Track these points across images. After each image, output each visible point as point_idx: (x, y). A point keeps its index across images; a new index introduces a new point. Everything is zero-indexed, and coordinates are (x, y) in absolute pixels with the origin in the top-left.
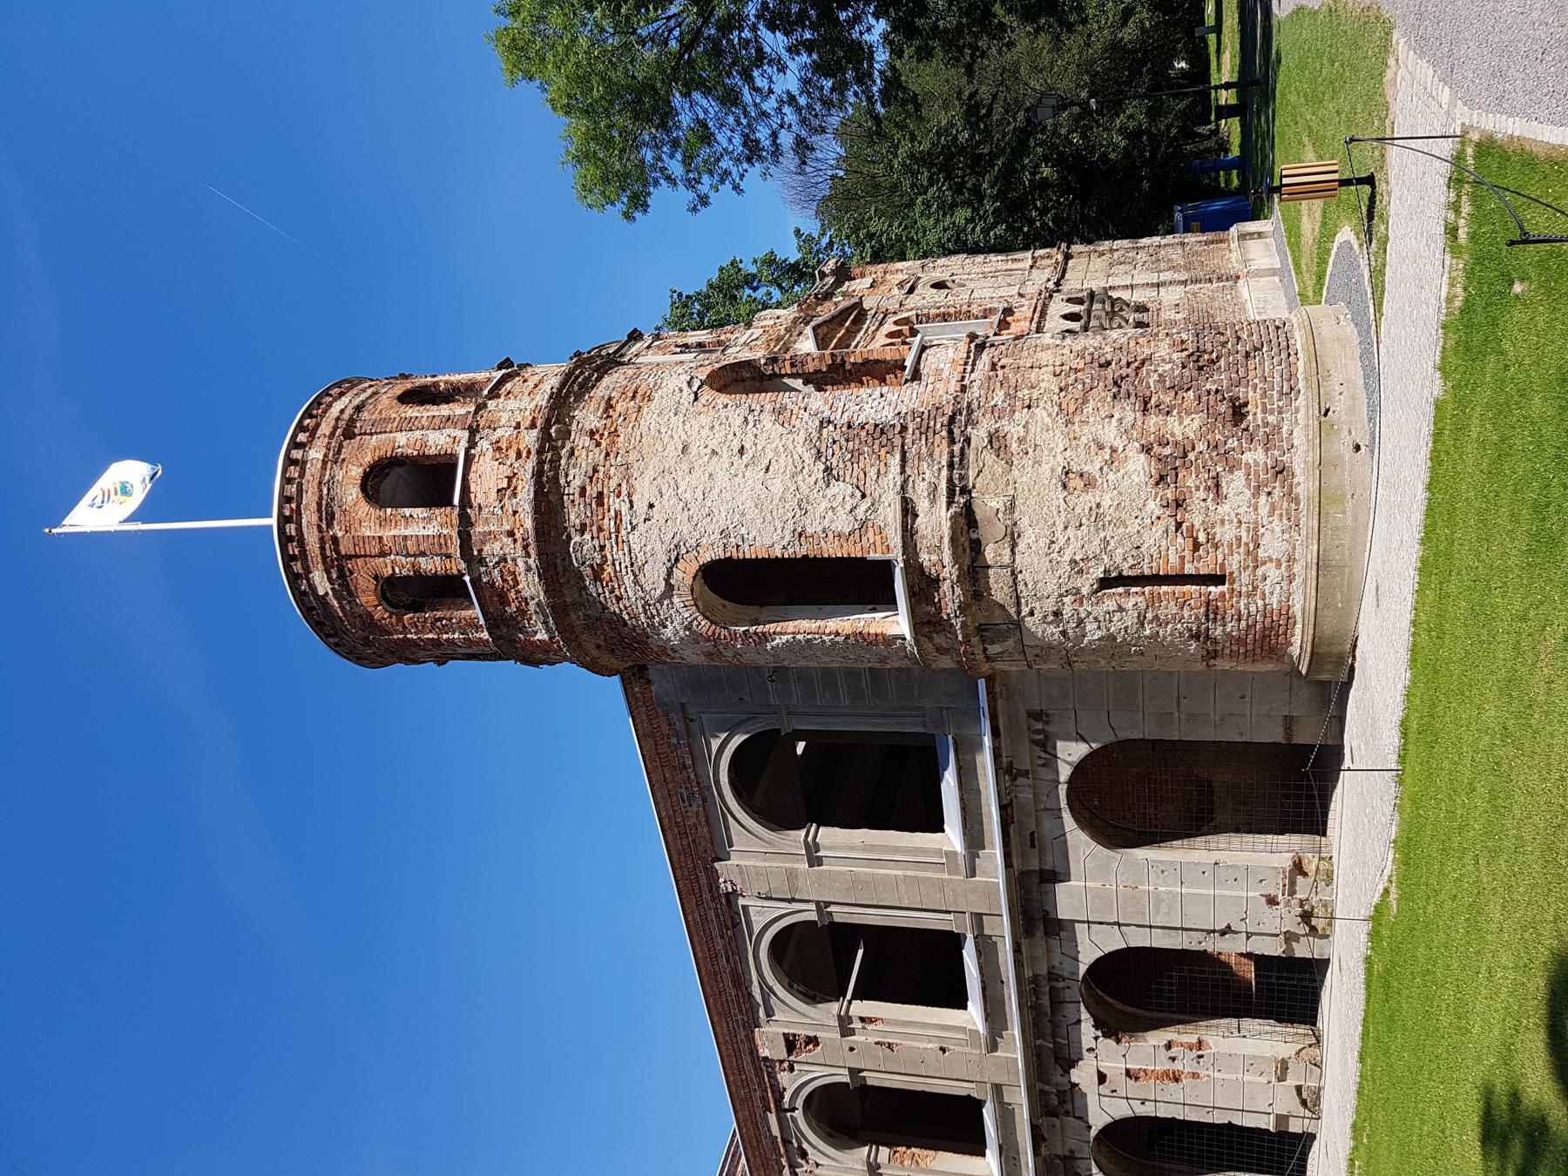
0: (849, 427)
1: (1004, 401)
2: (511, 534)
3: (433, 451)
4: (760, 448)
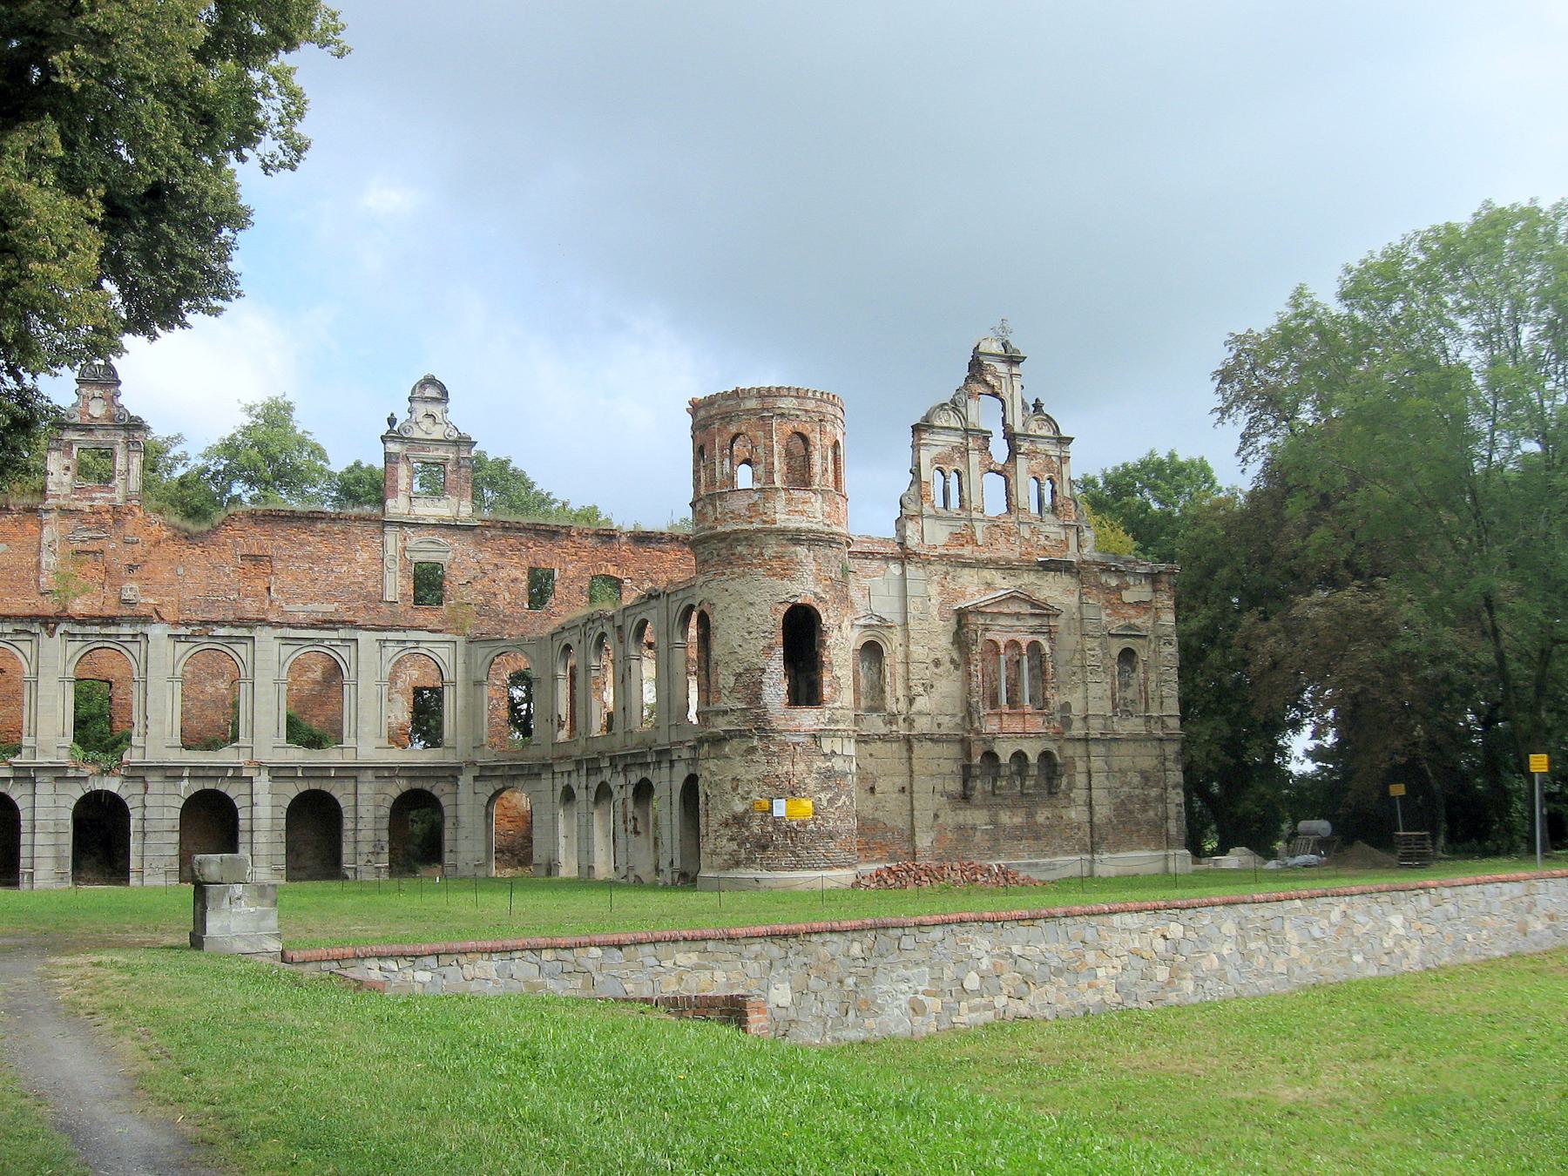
2: (716, 519)
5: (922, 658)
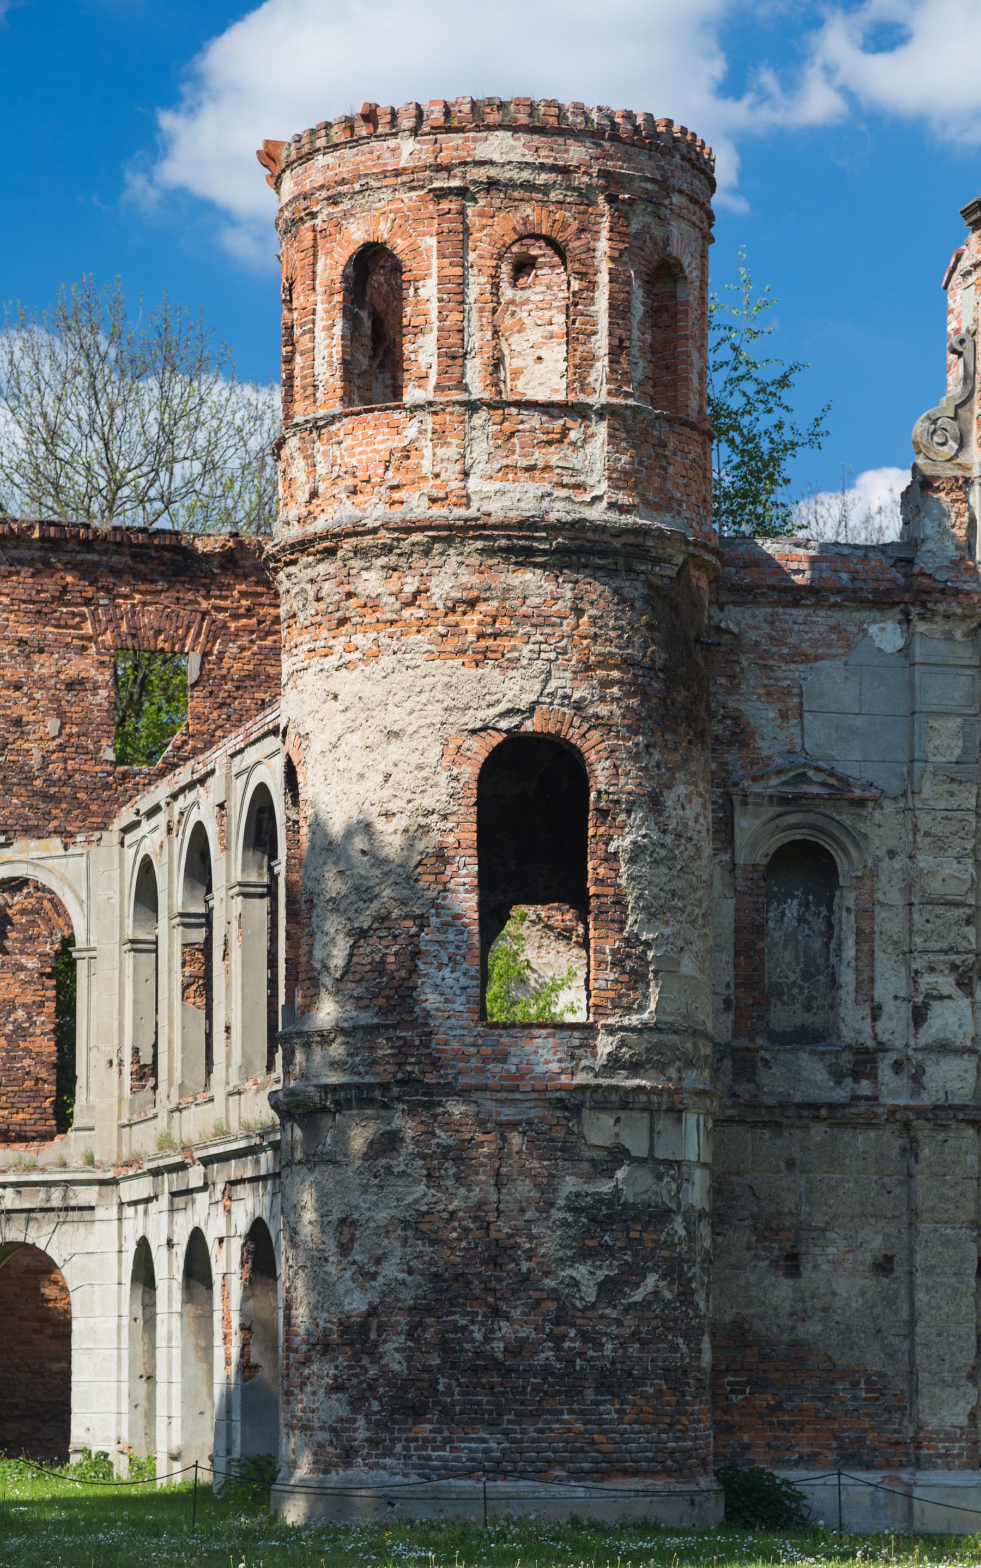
1: (438, 1145)
5: (953, 890)
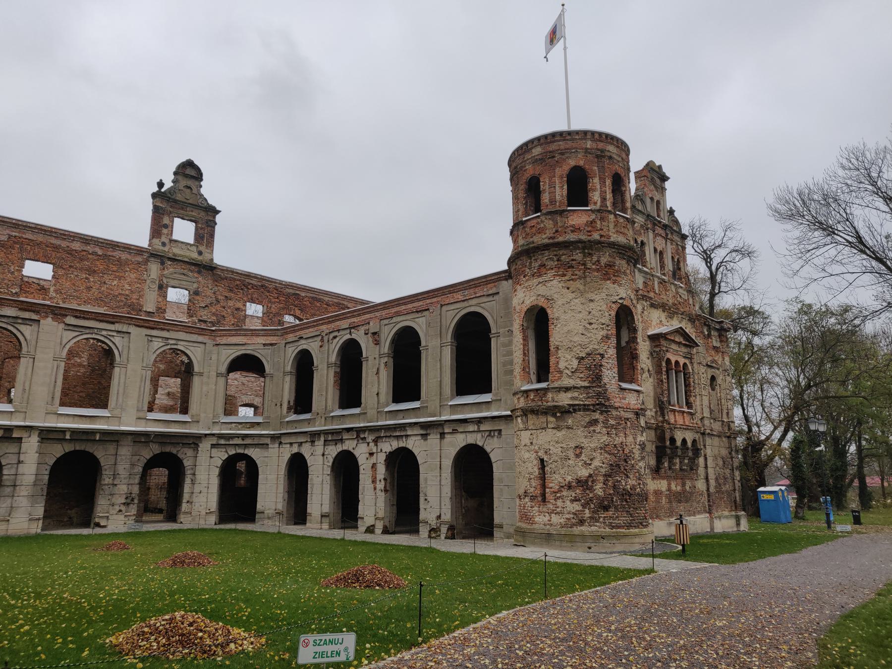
0: (600, 365)
3: (590, 195)
4: (592, 331)
